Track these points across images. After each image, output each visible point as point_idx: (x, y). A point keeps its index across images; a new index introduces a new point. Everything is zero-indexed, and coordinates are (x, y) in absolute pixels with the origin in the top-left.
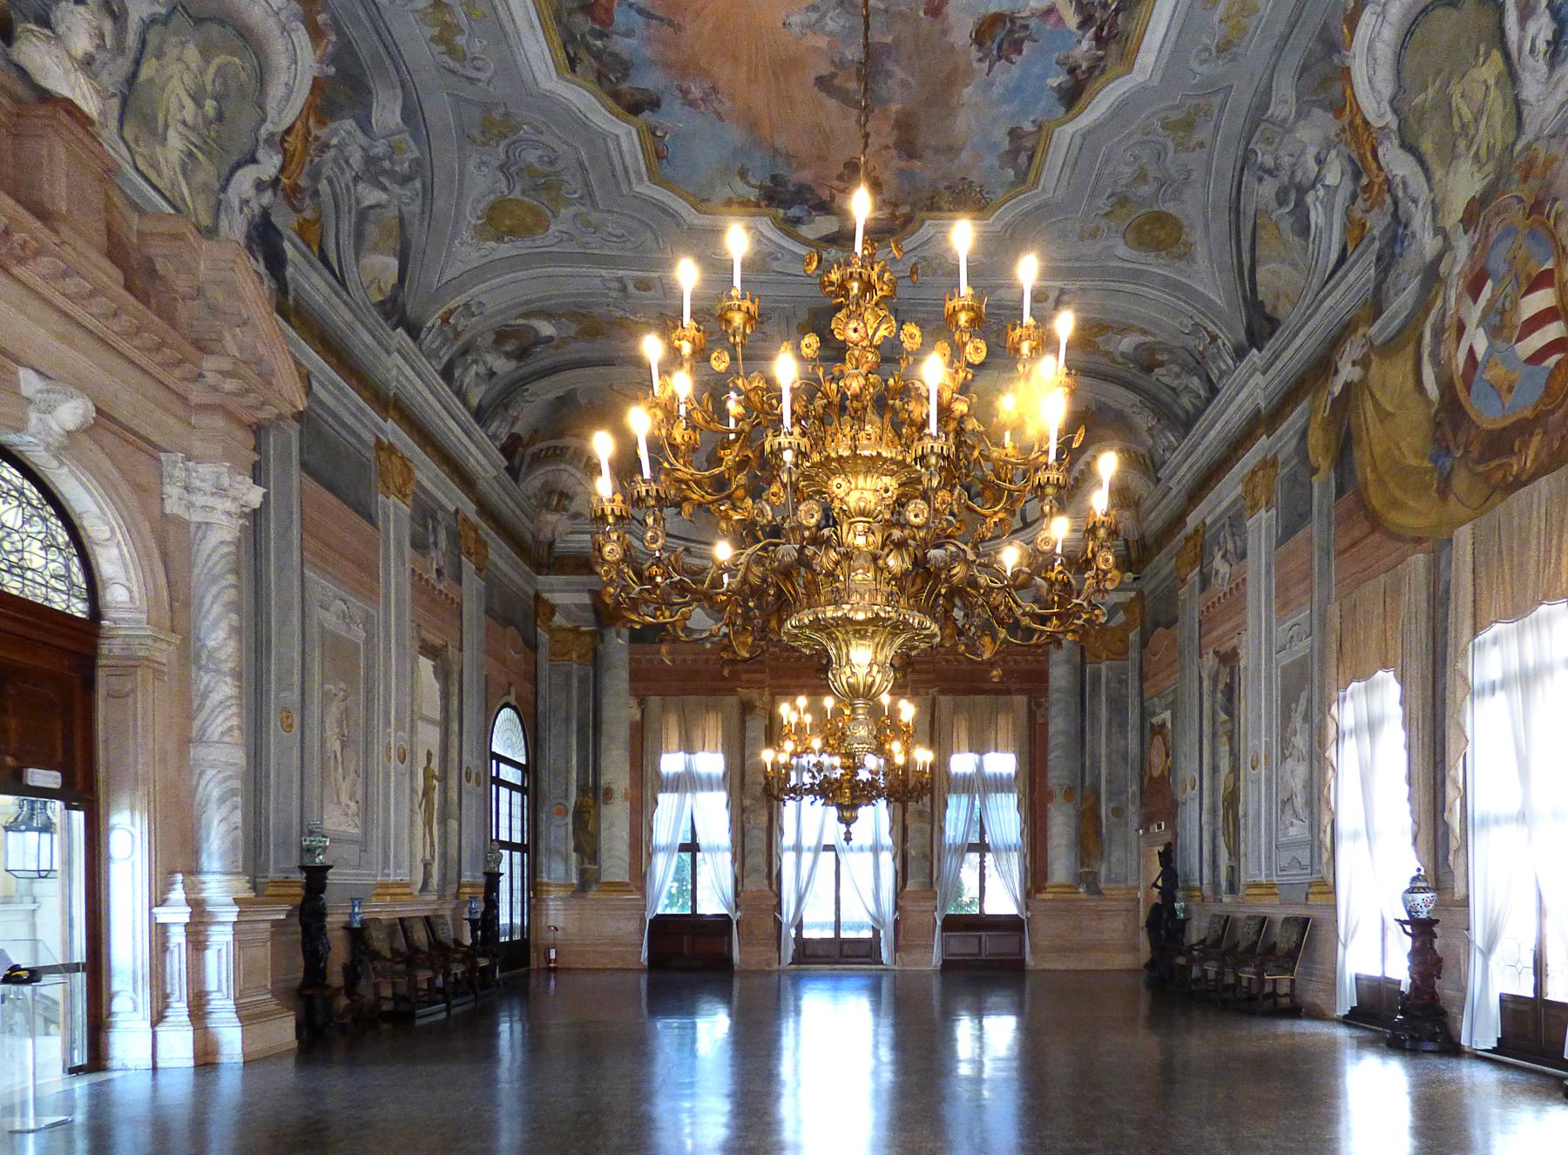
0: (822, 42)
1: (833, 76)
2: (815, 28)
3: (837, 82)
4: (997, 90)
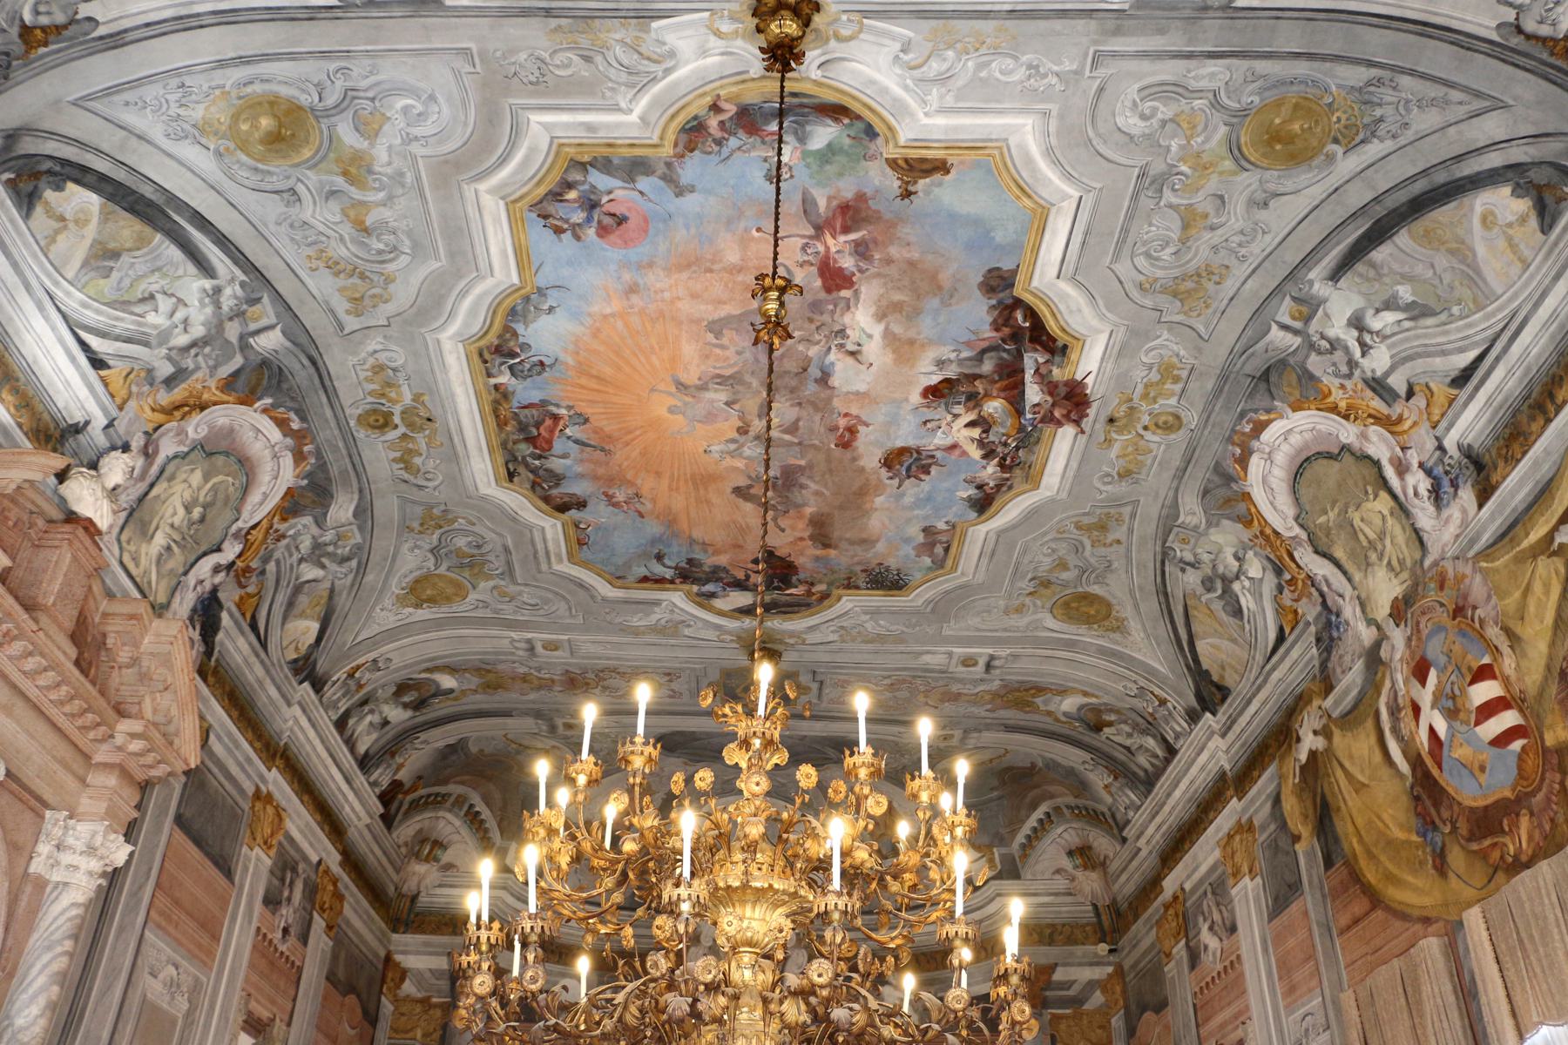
0: (740, 464)
1: (750, 487)
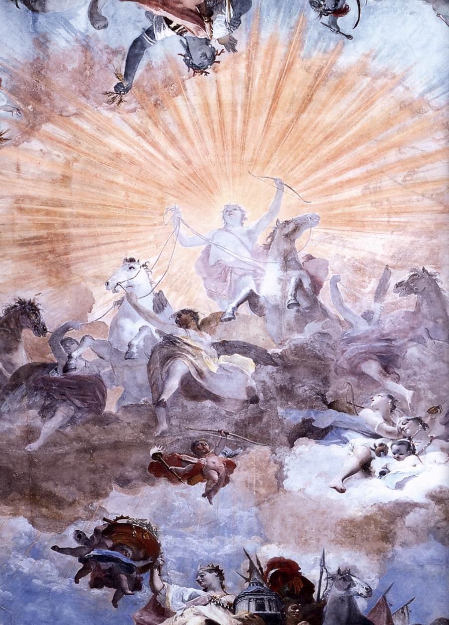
1: (40, 329)
2: (127, 301)
3: (27, 334)
4: (26, 565)
